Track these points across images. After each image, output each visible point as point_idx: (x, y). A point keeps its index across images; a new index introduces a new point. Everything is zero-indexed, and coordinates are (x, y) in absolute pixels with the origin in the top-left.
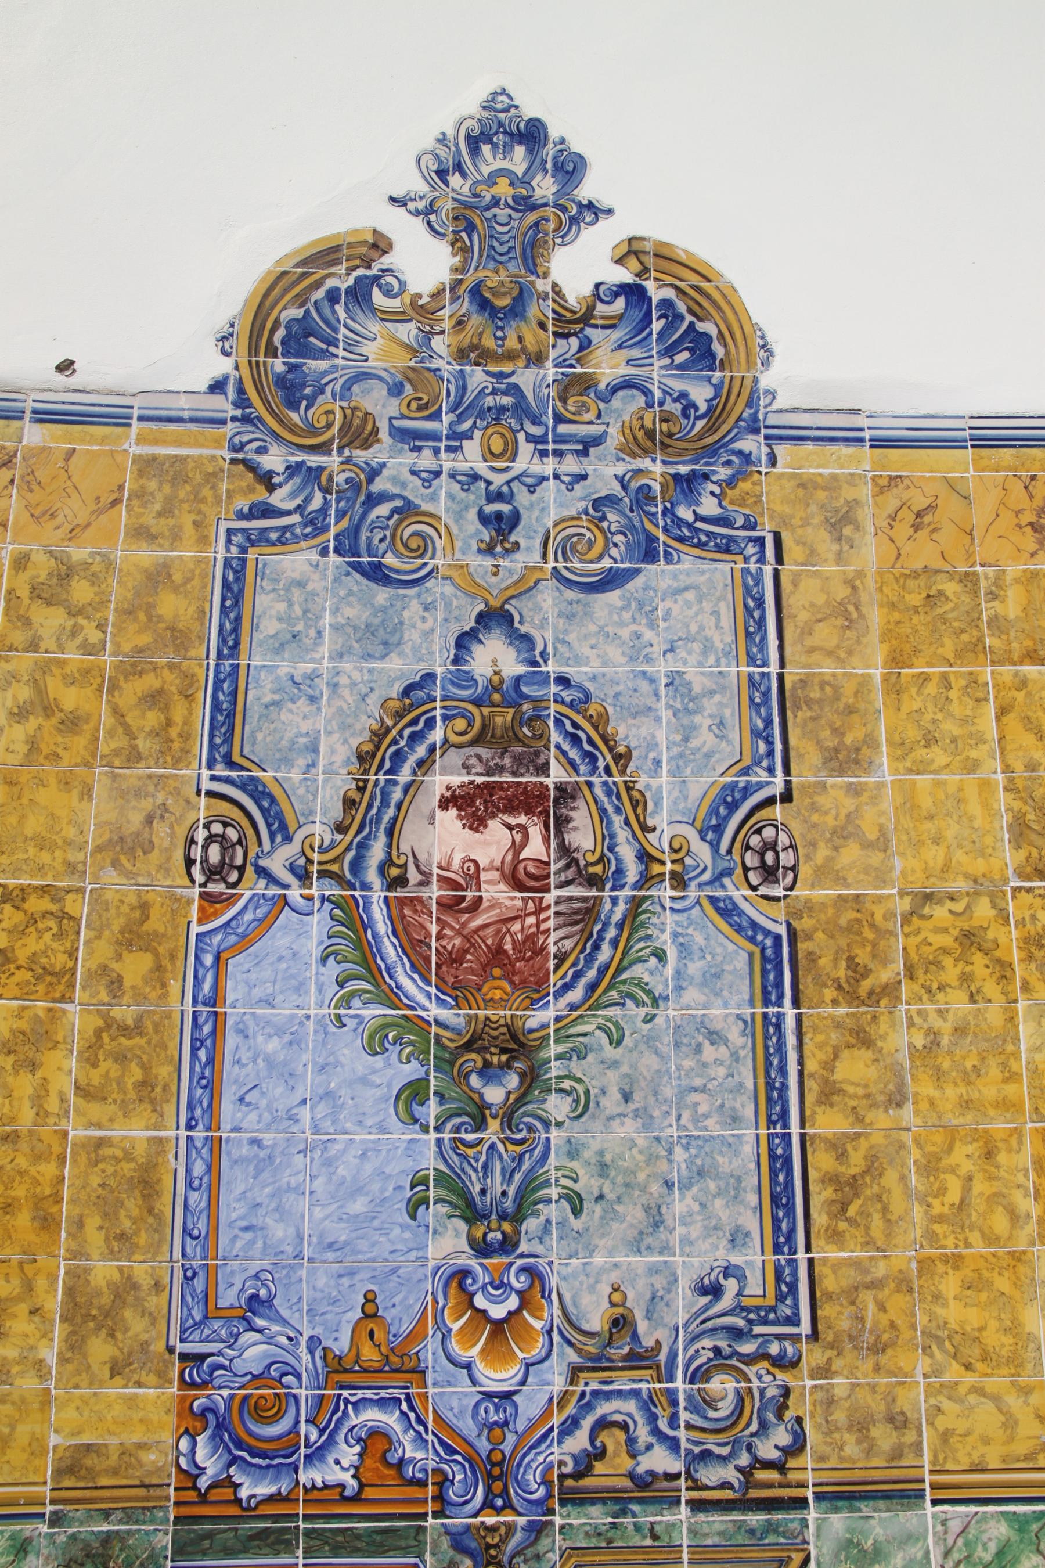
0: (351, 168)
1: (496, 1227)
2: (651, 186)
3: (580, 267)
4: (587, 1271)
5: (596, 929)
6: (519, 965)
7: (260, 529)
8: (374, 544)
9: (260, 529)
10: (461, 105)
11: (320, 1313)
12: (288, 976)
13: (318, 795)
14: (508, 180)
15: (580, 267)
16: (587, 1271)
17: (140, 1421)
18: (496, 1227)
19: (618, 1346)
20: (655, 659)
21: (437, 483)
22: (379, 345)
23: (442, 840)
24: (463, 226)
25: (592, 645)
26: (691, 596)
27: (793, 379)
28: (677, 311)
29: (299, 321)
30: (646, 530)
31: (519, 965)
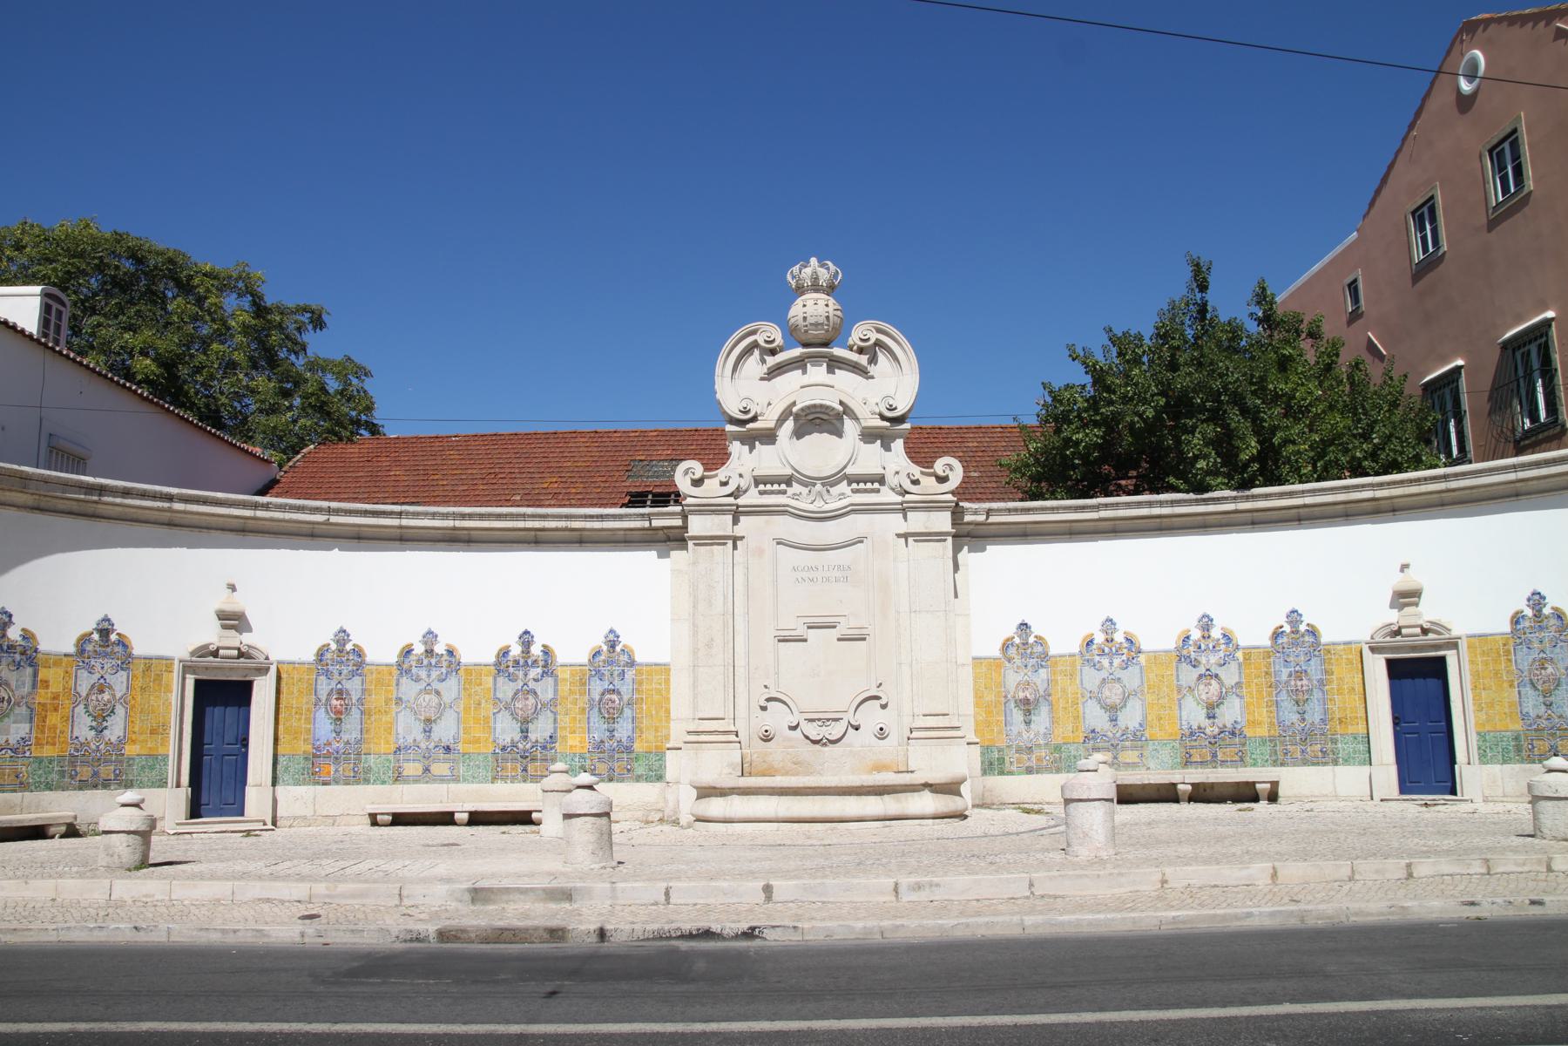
0: (327, 637)
1: (338, 733)
2: (356, 639)
3: (349, 647)
4: (345, 737)
5: (348, 710)
6: (340, 713)
7: (318, 674)
8: (328, 674)
9: (318, 674)
10: (337, 629)
11: (323, 741)
12: (321, 714)
13: (324, 699)
14: (342, 636)
15: (349, 647)
16: (345, 737)
17: (309, 748)
18: (338, 733)
19: (348, 743)
20: (354, 686)
21: (335, 669)
22: (329, 656)
23: (334, 702)
24: (338, 642)
25: (348, 685)
26: (357, 680)
27: (369, 658)
28: (358, 651)
29: (321, 653)
30: (353, 674)
31: (340, 713)
